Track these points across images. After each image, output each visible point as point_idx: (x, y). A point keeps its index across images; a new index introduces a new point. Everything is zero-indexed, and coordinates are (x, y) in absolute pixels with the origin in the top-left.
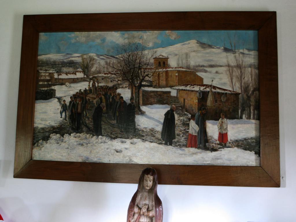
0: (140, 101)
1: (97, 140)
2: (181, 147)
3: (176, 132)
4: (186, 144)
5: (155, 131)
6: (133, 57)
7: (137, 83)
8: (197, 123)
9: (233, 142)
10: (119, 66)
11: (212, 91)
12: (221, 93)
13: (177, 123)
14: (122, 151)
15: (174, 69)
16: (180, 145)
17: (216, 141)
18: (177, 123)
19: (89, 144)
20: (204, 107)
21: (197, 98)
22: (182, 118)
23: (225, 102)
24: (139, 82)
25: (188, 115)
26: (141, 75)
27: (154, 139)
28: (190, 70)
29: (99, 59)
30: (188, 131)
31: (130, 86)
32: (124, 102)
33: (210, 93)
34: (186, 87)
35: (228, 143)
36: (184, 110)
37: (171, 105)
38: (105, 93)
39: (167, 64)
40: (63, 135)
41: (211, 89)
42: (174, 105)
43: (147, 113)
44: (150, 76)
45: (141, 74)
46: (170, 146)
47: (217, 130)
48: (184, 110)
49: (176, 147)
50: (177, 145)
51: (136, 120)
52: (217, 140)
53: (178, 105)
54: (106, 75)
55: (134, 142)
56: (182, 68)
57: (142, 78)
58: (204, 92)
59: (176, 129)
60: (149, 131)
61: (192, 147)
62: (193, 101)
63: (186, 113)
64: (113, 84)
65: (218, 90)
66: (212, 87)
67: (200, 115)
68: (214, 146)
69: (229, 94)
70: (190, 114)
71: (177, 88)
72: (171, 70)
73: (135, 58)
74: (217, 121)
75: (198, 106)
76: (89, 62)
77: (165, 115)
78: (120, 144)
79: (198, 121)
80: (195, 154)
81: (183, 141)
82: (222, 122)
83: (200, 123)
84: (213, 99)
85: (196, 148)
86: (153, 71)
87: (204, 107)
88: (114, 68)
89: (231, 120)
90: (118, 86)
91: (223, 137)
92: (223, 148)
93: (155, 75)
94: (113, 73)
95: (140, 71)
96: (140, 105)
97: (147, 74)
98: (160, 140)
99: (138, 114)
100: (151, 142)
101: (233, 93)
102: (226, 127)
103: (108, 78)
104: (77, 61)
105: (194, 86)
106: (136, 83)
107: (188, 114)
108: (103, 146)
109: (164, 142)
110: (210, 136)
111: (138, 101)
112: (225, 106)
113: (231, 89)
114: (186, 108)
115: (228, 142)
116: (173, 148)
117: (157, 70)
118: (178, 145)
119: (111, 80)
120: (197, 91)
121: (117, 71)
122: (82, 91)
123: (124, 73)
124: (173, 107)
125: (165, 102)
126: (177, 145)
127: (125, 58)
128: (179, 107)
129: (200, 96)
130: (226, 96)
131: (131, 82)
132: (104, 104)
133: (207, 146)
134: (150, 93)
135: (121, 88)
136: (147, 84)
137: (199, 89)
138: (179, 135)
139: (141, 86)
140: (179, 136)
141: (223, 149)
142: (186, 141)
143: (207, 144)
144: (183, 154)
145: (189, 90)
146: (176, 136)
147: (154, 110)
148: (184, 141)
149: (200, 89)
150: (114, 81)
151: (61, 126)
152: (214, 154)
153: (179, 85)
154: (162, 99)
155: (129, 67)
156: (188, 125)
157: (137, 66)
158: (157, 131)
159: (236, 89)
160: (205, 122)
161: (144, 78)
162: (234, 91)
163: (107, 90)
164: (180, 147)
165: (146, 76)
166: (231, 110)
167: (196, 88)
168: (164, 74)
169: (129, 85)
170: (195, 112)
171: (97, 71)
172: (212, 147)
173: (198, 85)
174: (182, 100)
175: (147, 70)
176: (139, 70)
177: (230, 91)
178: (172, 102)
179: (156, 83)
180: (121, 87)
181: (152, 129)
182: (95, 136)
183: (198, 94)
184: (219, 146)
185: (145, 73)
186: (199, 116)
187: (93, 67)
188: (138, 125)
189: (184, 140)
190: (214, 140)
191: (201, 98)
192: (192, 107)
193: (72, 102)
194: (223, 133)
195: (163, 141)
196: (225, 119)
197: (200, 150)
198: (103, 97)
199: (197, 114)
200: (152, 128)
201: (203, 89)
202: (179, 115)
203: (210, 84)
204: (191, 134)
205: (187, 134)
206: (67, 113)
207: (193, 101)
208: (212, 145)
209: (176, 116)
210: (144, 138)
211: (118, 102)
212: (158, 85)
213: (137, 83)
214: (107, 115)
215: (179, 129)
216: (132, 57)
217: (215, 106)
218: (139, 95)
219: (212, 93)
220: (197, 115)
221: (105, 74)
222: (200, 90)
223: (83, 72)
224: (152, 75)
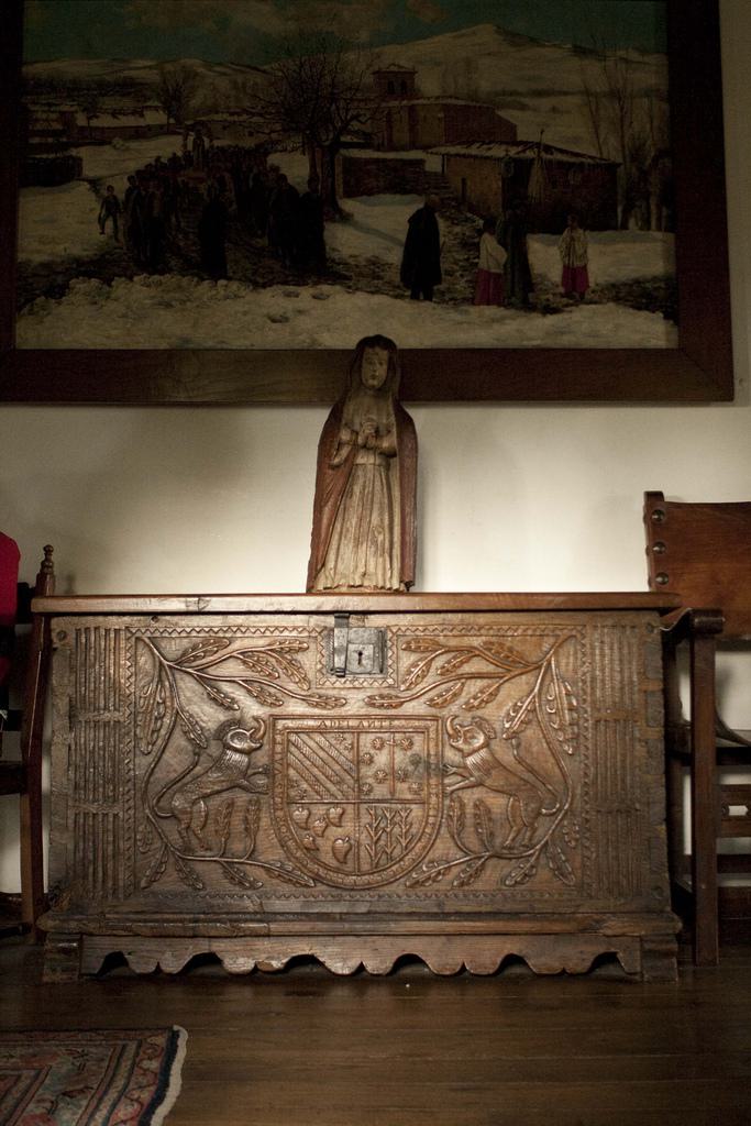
1: (214, 292)
5: (383, 265)
8: (502, 242)
11: (540, 158)
17: (557, 286)
18: (444, 243)
19: (188, 304)
22: (457, 229)
28: (478, 105)
40: (108, 282)
41: (539, 152)
42: (436, 194)
43: (358, 217)
46: (428, 303)
47: (558, 257)
50: (446, 298)
51: (326, 234)
52: (560, 283)
56: (457, 98)
61: (488, 304)
63: (469, 215)
65: (558, 156)
69: (589, 165)
70: (482, 217)
71: (443, 150)
74: (557, 237)
82: (572, 239)
85: (499, 304)
92: (577, 306)
96: (337, 197)
98: (398, 287)
99: (333, 220)
100: (372, 293)
102: (582, 251)
109: (408, 293)
110: (540, 275)
113: (594, 153)
115: (589, 290)
116: (434, 308)
120: (499, 159)
126: (446, 298)
133: (531, 300)
138: (450, 273)
142: (473, 288)
143: (530, 295)
145: (475, 157)
146: (443, 276)
152: (551, 320)
154: (400, 180)
156: (477, 247)
162: (601, 159)
167: (498, 151)
172: (544, 303)
173: (502, 143)
182: (207, 282)
188: (334, 250)
196: (581, 231)
197: (511, 312)
201: (518, 153)
203: (535, 138)
207: (489, 186)
208: (544, 297)
209: (442, 225)
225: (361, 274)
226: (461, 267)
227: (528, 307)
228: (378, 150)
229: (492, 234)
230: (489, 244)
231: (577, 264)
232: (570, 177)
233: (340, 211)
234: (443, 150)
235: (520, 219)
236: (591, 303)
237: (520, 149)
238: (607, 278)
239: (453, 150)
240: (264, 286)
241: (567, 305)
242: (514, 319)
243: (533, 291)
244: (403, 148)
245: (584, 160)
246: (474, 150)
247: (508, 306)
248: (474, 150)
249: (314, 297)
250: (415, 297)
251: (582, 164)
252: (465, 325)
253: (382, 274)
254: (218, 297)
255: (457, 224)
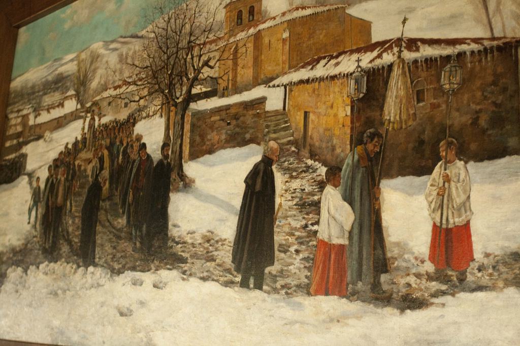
0: (184, 148)
1: (84, 280)
2: (291, 294)
3: (275, 238)
4: (306, 280)
5: (217, 242)
6: (178, 21)
7: (180, 94)
8: (348, 198)
9: (497, 262)
10: (145, 56)
11: (403, 61)
12: (441, 57)
13: (280, 205)
14: (131, 311)
15: (278, 21)
16: (289, 288)
17: (423, 262)
18: (280, 205)
19: (67, 292)
20: (372, 130)
21: (348, 101)
22: (296, 184)
23: (455, 93)
24: (185, 89)
25: (315, 171)
26: (192, 68)
27: (211, 269)
28: (327, 8)
29: (108, 52)
30: (316, 232)
31: (164, 107)
32: (149, 156)
33: (395, 68)
34: (312, 69)
35: (476, 271)
36: (305, 152)
37: (267, 142)
38: (110, 142)
39: (260, 12)
40: (25, 271)
41: (400, 52)
42: (275, 139)
43: (199, 184)
44: (211, 63)
45: (191, 65)
46: (257, 292)
47: (426, 213)
48: (305, 152)
49: (276, 296)
50: (278, 285)
51: (171, 209)
52: (427, 258)
53: (285, 140)
54: (118, 90)
55: (161, 282)
56: (303, 8)
57: (193, 75)
58: (374, 69)
59: (278, 226)
60: (199, 242)
61: (327, 294)
62: (335, 115)
63: (310, 162)
64: (129, 111)
65: (427, 51)
66: (404, 44)
67: (359, 161)
68: (414, 285)
69: (473, 52)
70: (325, 164)
71: (285, 79)
72: (271, 27)
73: (181, 21)
74: (424, 178)
75: (352, 129)
76: (88, 66)
77: (245, 181)
78: (129, 289)
79: (352, 189)
80: (338, 321)
81: (297, 271)
82: (447, 179)
83: (357, 193)
84: (406, 88)
85: (342, 295)
86: (222, 44)
87: (372, 130)
88: (135, 67)
89: (486, 163)
90: (139, 115)
91: (451, 243)
92: (453, 295)
93: (226, 55)
94: (130, 80)
95: (189, 56)
96: (183, 161)
97: (206, 59)
98: (228, 271)
99: (177, 190)
100: (204, 279)
101: (492, 48)
102: (463, 197)
103: (120, 98)
104: (68, 71)
105: (340, 59)
106: (178, 94)
107: (317, 165)
108: (95, 296)
109: (238, 279)
110: (398, 244)
111: (178, 149)
112: (458, 110)
113: (480, 32)
114: (310, 145)
115: (474, 265)
116: (264, 300)
117: (232, 40)
118: (283, 287)
119: (126, 100)
120: (348, 75)
121: (140, 73)
122: (70, 146)
123: (154, 73)
124: (272, 149)
125: (248, 136)
126: (278, 285)
127: (160, 30)
128: (288, 147)
129: (358, 90)
130: (461, 67)
131: (166, 96)
132: (106, 173)
133: (385, 287)
134: (210, 117)
135: (145, 118)
136: (204, 90)
137: (356, 64)
138: (284, 249)
139: (191, 98)
140: (285, 252)
141: (449, 298)
142: (309, 269)
143: (384, 278)
144: (297, 322)
145: (321, 79)
146: (277, 253)
147: (217, 170)
148: (299, 269)
149: (360, 64)
150: (131, 102)
151: (26, 245)
152: (413, 317)
153: (290, 68)
154: (241, 127)
155: (167, 53)
156: (317, 205)
157: (184, 43)
158: (221, 240)
159: (504, 26)
160: (379, 189)
161: (199, 72)
162: (493, 39)
163: (115, 134)
164: (287, 293)
165: (203, 66)
166: (483, 122)
167: (348, 64)
168: (250, 45)
169: (163, 104)
170: (342, 155)
171: (102, 85)
172: (404, 291)
173: (352, 52)
174: (298, 117)
175: (208, 46)
176: (187, 55)
177: (476, 41)
178: (268, 132)
179: (228, 80)
180: (144, 115)
181: (208, 234)
182: (82, 268)
183: (353, 82)
184: (434, 283)
185: (202, 58)
186: (355, 167)
187: (94, 78)
188: (175, 226)
189: (302, 266)
190: (413, 261)
191: (362, 95)
192: (330, 139)
193: (51, 180)
194: (450, 226)
195: (235, 273)
196: (460, 164)
197: (355, 306)
198: (106, 152)
199: (349, 161)
200: (209, 231)
201: (371, 62)
202: (287, 176)
203: (394, 35)
204: (326, 240)
205: (311, 243)
206: (40, 210)
207: (333, 116)
208: (403, 281)
209: (279, 179)
210: (186, 267)
211: (134, 161)
212: (232, 85)
213: (181, 95)
214: (110, 205)
215: (287, 223)
216: (175, 20)
217: (415, 114)
218: (182, 128)
219: (403, 67)
220: (348, 164)
221: (115, 88)
222: (359, 66)
223: (75, 97)
224: (217, 58)
225: (195, 256)
226: (298, 238)
227: (381, 297)
228: (223, 96)
229: (336, 186)
230: (333, 200)
231: (456, 220)
232: (444, 80)
233: (182, 176)
234: (285, 79)
235: (377, 156)
236: (480, 288)
237: (375, 53)
238: (501, 243)
239: (296, 76)
240: (119, 272)
241: (435, 295)
242: (358, 317)
243: (386, 271)
244: (247, 88)
245: (464, 47)
246: (320, 71)
247: (352, 296)
248: (320, 71)
249: (155, 286)
250: (244, 284)
251: (461, 55)
252: (297, 326)
253: (215, 253)
254: (87, 285)
255: (296, 178)
